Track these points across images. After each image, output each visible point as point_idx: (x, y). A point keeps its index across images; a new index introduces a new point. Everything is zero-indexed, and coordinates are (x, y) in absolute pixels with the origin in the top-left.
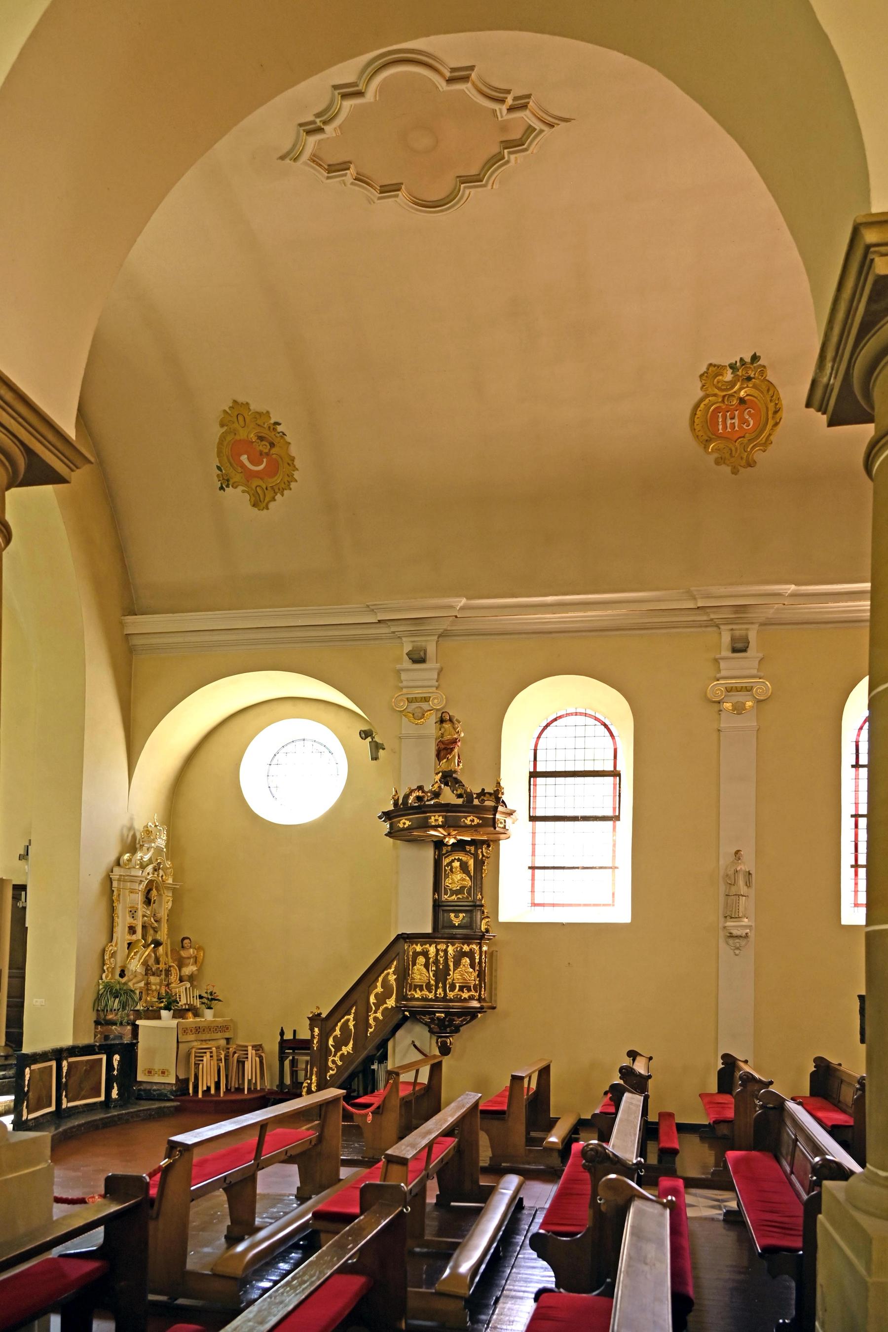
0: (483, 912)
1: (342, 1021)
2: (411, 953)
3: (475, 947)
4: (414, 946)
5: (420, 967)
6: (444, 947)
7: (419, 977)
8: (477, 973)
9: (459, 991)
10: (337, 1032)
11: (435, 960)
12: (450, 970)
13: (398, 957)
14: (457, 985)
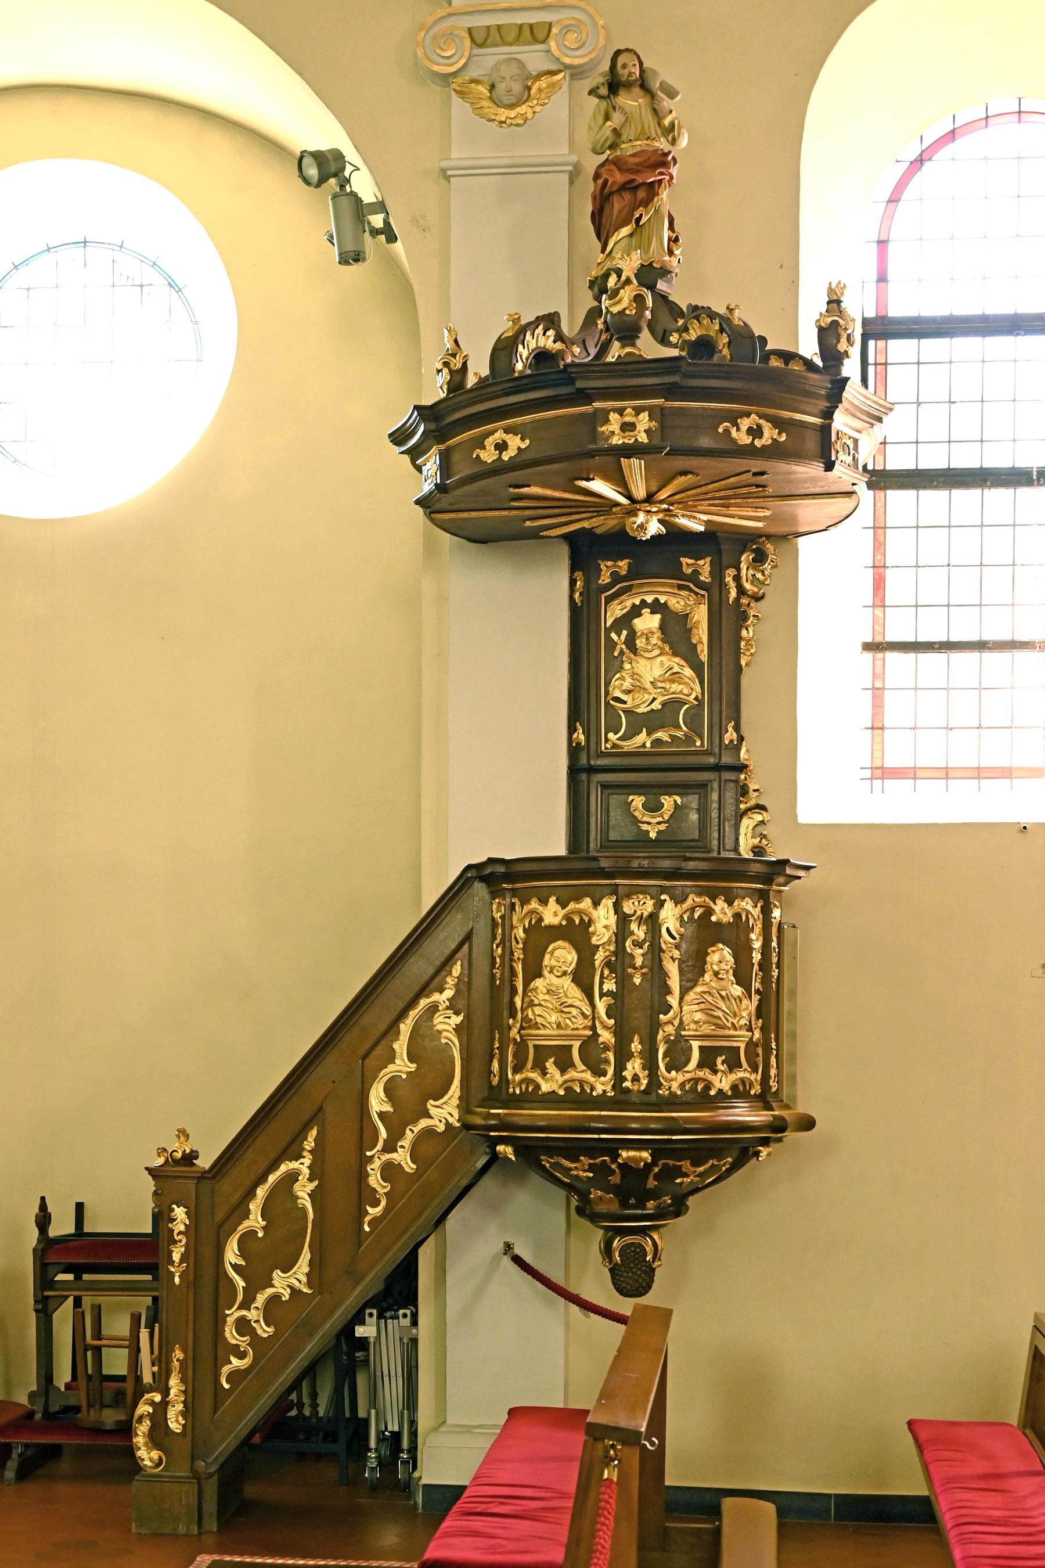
0: (744, 791)
1: (272, 1179)
2: (520, 933)
3: (749, 908)
4: (534, 904)
5: (556, 981)
6: (649, 906)
7: (554, 1018)
8: (756, 998)
9: (700, 1066)
10: (255, 1221)
11: (615, 953)
12: (669, 992)
13: (466, 947)
14: (695, 1045)
